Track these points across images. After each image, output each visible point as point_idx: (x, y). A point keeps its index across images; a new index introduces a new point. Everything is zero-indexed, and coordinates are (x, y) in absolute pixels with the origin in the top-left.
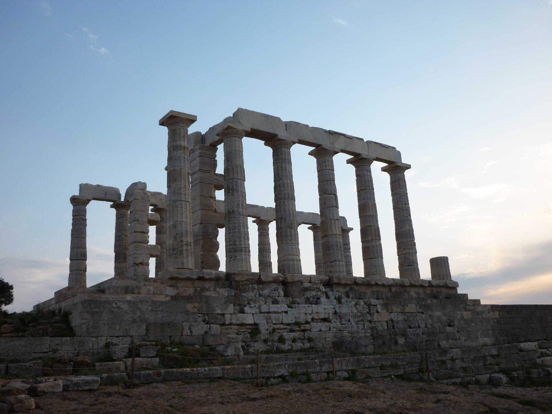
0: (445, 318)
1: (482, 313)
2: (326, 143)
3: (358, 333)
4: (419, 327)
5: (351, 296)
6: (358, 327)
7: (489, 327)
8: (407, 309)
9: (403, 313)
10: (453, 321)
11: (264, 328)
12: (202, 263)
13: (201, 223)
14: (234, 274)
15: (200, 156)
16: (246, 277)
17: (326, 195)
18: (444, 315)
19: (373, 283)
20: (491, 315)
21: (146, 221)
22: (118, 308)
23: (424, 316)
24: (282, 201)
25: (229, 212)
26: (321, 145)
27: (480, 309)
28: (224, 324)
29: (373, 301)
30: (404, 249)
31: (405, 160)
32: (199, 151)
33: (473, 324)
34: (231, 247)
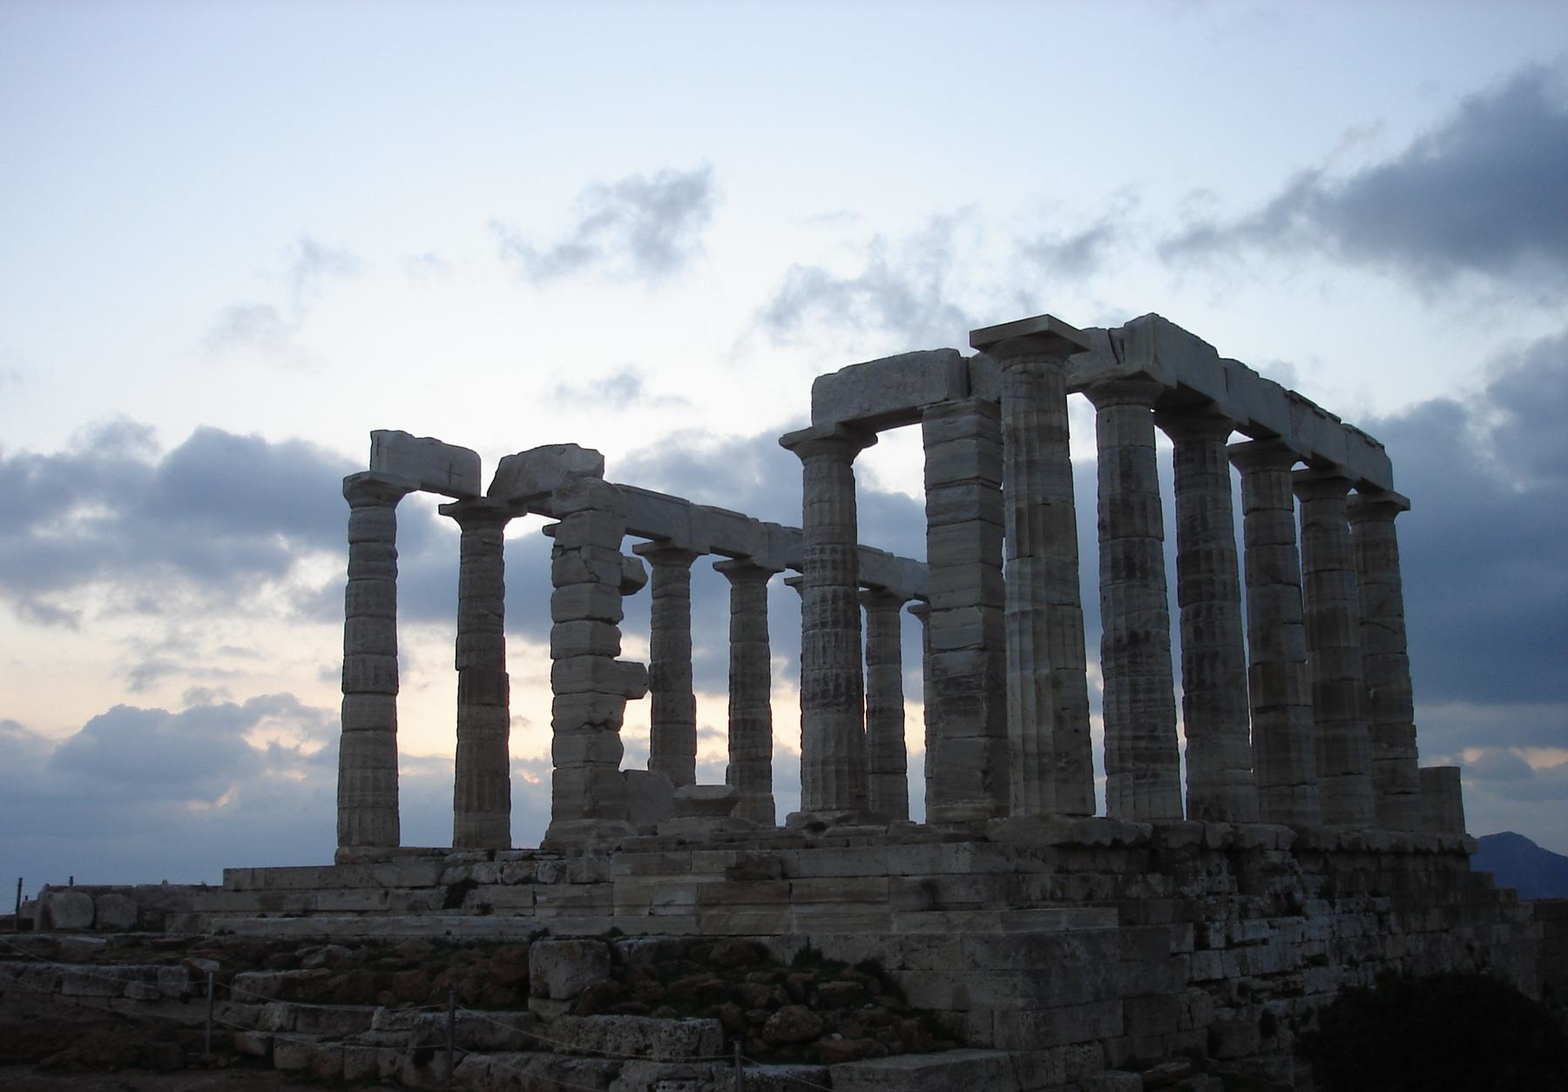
12: (985, 773)
13: (983, 649)
14: (1165, 829)
15: (978, 435)
17: (1279, 587)
19: (1364, 847)
21: (618, 582)
22: (1072, 955)
24: (1215, 602)
25: (1134, 638)
26: (1278, 436)
29: (1382, 903)
30: (1391, 746)
31: (1401, 485)
32: (974, 418)
34: (1143, 744)
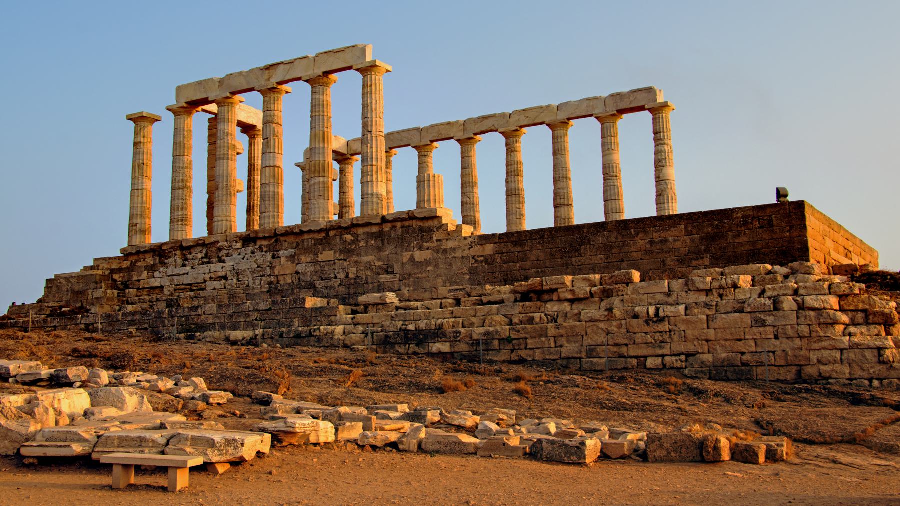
0: (380, 263)
1: (454, 250)
2: (263, 83)
3: (254, 288)
4: (336, 278)
5: (265, 250)
6: (254, 283)
7: (465, 270)
8: (321, 258)
9: (315, 263)
10: (392, 267)
11: (166, 291)
16: (170, 246)
18: (379, 260)
19: (297, 231)
20: (477, 251)
23: (346, 264)
27: (450, 244)
28: (138, 289)
33: (430, 268)
